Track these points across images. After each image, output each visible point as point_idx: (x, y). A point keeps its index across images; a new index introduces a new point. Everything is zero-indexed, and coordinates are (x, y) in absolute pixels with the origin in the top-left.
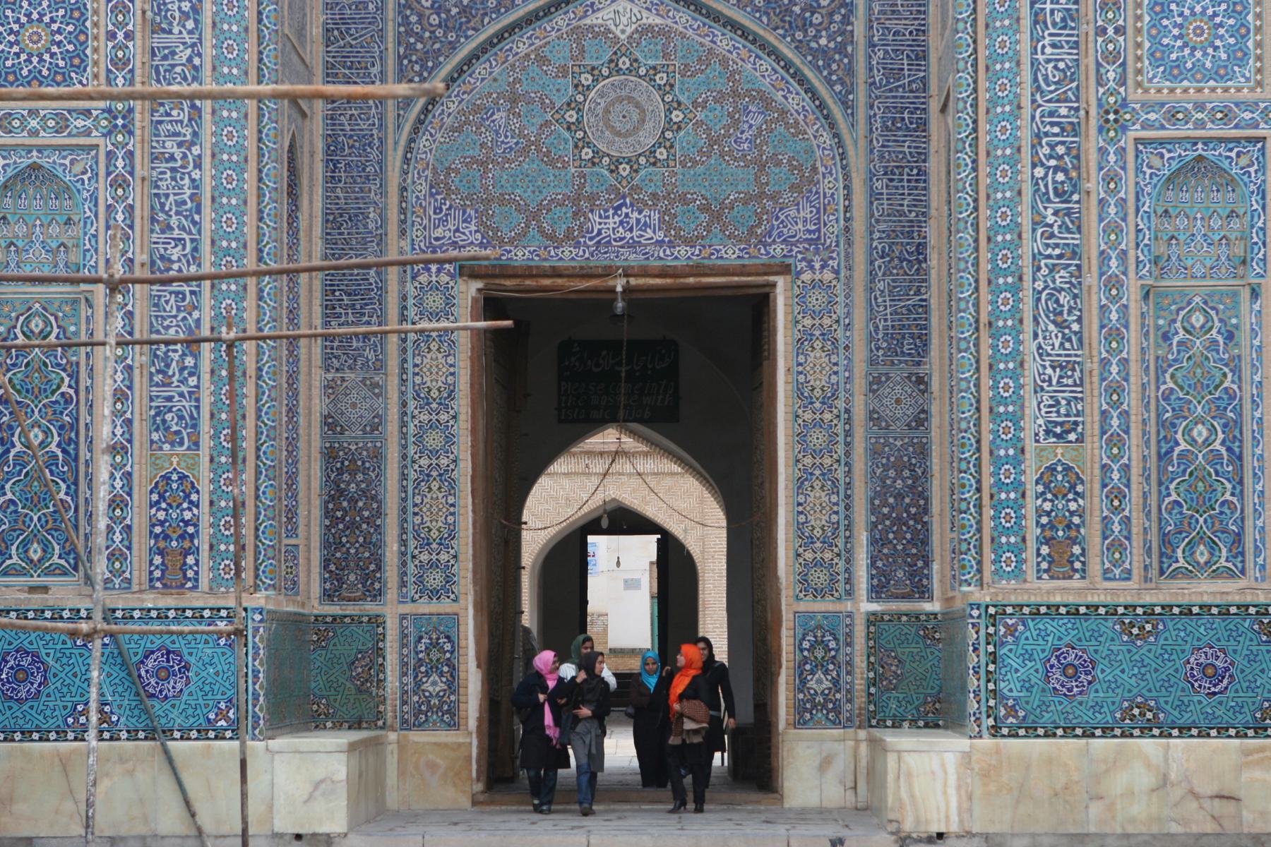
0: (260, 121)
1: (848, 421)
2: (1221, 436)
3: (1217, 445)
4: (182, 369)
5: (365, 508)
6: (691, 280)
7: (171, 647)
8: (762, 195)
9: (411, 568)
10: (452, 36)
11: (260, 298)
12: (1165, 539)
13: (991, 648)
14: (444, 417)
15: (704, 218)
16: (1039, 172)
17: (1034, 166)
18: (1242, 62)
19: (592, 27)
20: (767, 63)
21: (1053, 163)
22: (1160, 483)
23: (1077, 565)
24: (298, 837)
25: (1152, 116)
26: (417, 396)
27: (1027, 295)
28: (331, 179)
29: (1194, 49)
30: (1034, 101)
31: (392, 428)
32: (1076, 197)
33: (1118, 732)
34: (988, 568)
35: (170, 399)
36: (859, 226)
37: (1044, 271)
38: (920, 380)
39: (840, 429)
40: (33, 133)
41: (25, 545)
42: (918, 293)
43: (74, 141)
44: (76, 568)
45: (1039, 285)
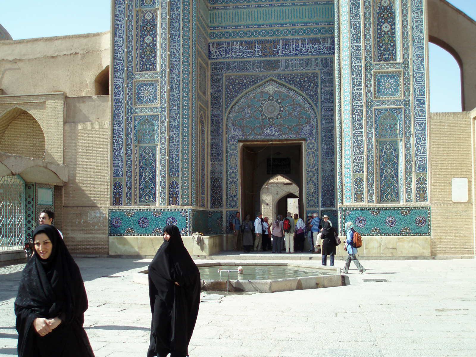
0: (192, 109)
1: (317, 171)
2: (393, 172)
3: (392, 174)
4: (176, 160)
5: (219, 189)
6: (285, 142)
7: (173, 217)
8: (299, 124)
10: (236, 94)
11: (192, 145)
12: (381, 194)
13: (344, 217)
14: (235, 171)
15: (288, 129)
16: (354, 116)
17: (353, 115)
18: (397, 92)
19: (264, 91)
20: (300, 98)
21: (357, 114)
22: (380, 182)
23: (363, 199)
24: (199, 256)
25: (378, 103)
26: (230, 167)
28: (212, 123)
29: (387, 89)
30: (353, 101)
31: (224, 173)
32: (362, 121)
33: (371, 235)
35: (173, 166)
36: (319, 131)
37: (355, 137)
38: (332, 162)
39: (316, 172)
41: (145, 196)
42: (332, 144)
43: (154, 114)
45: (354, 140)
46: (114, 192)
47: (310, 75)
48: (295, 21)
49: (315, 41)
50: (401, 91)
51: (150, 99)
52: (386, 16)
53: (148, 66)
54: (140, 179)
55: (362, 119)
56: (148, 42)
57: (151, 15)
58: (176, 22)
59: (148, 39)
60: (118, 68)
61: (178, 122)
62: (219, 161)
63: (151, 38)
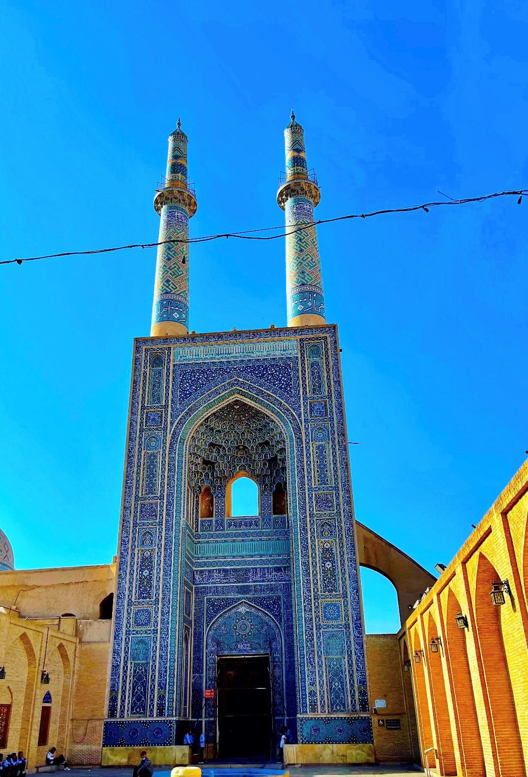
3: (340, 686)
9: (207, 711)
12: (331, 704)
16: (307, 637)
18: (339, 617)
27: (305, 659)
34: (302, 711)
40: (141, 634)
44: (145, 713)
46: (110, 705)
47: (275, 598)
48: (262, 553)
49: (278, 569)
50: (342, 616)
51: (145, 623)
52: (328, 556)
53: (145, 595)
54: (133, 693)
55: (313, 640)
56: (146, 575)
57: (149, 553)
58: (169, 559)
59: (146, 573)
60: (121, 596)
61: (167, 642)
62: (200, 673)
63: (148, 572)
